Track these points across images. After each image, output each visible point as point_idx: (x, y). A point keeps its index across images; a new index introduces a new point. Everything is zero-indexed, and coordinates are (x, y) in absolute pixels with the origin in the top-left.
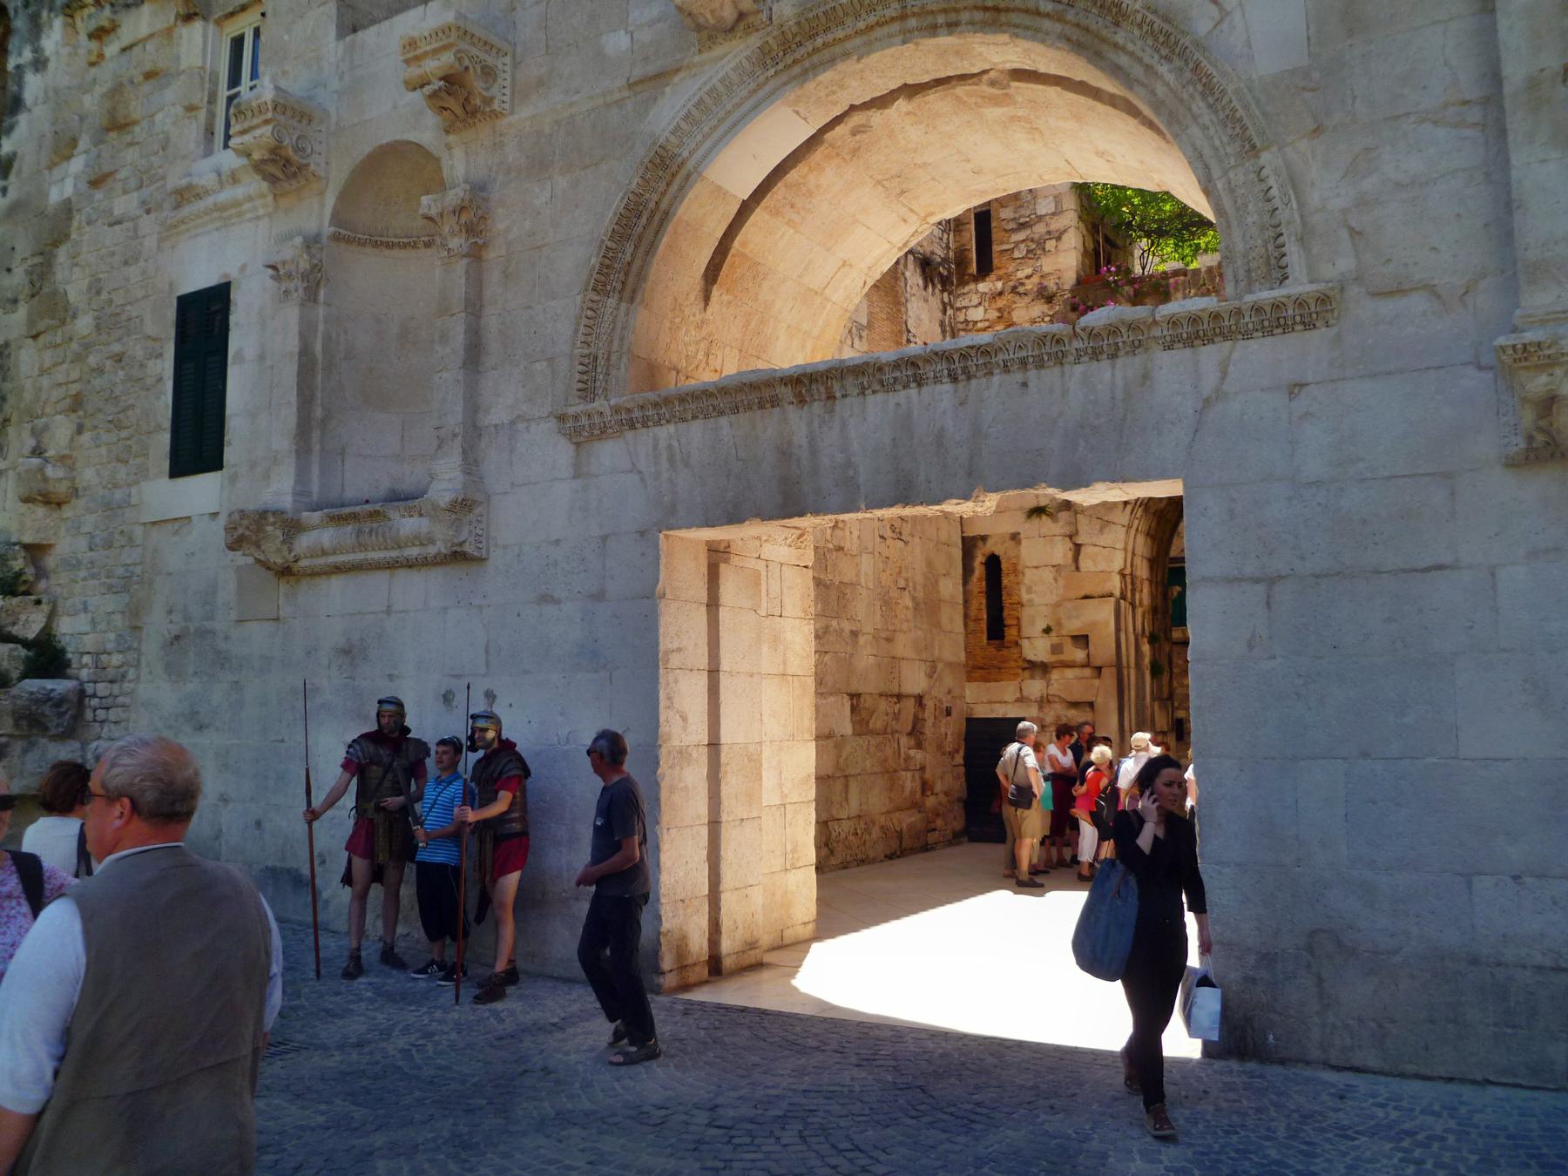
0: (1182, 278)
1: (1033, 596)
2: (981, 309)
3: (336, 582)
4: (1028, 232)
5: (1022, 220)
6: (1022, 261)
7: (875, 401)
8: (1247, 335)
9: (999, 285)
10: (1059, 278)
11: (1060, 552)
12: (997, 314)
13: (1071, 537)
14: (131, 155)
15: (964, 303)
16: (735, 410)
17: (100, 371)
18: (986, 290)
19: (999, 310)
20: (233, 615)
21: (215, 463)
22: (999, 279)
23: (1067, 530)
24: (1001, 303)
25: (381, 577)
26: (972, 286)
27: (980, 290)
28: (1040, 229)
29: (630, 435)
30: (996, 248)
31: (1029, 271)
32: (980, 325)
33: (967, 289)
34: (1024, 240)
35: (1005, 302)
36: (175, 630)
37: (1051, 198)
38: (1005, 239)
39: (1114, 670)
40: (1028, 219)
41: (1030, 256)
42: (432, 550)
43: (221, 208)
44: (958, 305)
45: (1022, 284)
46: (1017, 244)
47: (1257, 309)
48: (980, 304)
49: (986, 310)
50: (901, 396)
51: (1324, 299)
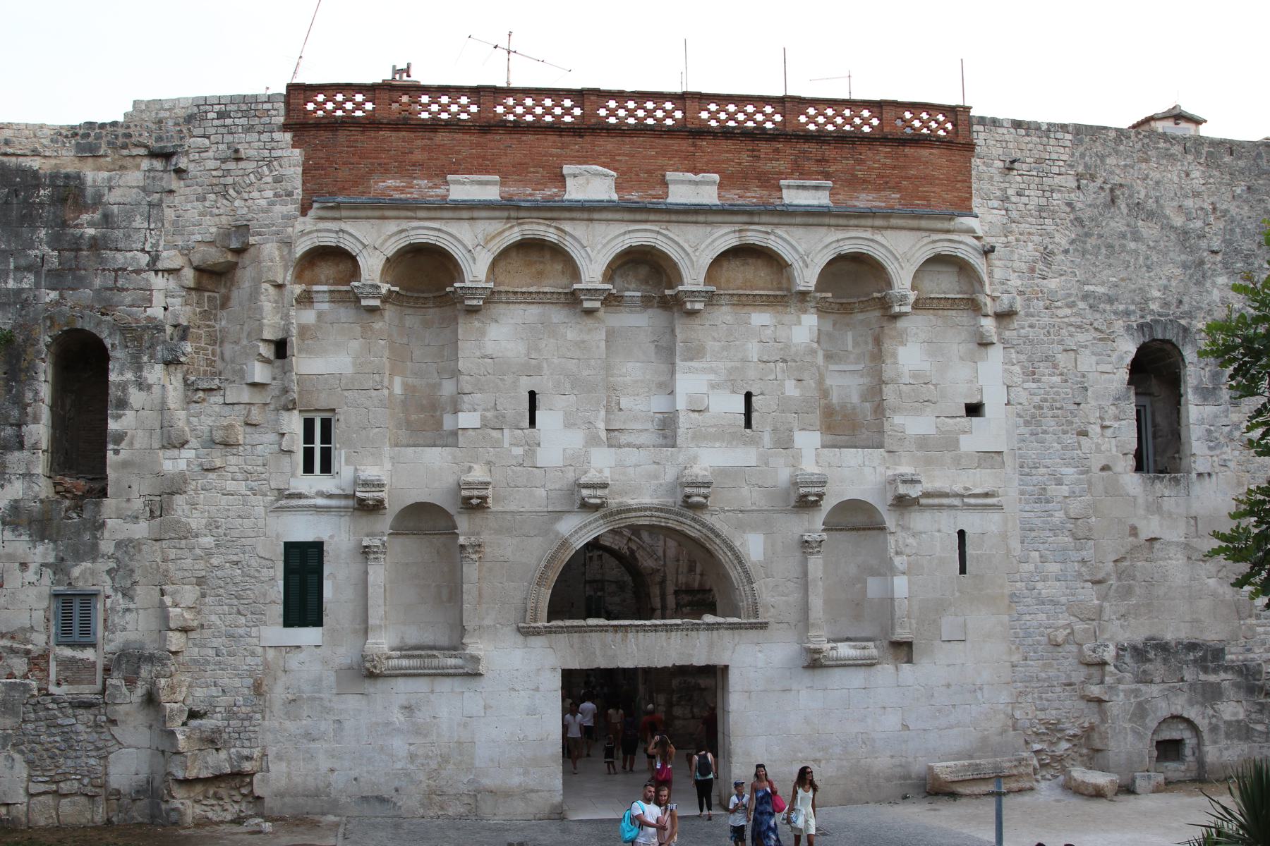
3: (400, 681)
7: (641, 635)
8: (746, 629)
14: (233, 460)
16: (591, 631)
17: (219, 567)
20: (334, 691)
21: (319, 623)
25: (426, 679)
36: (291, 697)
42: (461, 671)
43: (316, 506)
47: (750, 624)
50: (650, 634)
51: (766, 623)
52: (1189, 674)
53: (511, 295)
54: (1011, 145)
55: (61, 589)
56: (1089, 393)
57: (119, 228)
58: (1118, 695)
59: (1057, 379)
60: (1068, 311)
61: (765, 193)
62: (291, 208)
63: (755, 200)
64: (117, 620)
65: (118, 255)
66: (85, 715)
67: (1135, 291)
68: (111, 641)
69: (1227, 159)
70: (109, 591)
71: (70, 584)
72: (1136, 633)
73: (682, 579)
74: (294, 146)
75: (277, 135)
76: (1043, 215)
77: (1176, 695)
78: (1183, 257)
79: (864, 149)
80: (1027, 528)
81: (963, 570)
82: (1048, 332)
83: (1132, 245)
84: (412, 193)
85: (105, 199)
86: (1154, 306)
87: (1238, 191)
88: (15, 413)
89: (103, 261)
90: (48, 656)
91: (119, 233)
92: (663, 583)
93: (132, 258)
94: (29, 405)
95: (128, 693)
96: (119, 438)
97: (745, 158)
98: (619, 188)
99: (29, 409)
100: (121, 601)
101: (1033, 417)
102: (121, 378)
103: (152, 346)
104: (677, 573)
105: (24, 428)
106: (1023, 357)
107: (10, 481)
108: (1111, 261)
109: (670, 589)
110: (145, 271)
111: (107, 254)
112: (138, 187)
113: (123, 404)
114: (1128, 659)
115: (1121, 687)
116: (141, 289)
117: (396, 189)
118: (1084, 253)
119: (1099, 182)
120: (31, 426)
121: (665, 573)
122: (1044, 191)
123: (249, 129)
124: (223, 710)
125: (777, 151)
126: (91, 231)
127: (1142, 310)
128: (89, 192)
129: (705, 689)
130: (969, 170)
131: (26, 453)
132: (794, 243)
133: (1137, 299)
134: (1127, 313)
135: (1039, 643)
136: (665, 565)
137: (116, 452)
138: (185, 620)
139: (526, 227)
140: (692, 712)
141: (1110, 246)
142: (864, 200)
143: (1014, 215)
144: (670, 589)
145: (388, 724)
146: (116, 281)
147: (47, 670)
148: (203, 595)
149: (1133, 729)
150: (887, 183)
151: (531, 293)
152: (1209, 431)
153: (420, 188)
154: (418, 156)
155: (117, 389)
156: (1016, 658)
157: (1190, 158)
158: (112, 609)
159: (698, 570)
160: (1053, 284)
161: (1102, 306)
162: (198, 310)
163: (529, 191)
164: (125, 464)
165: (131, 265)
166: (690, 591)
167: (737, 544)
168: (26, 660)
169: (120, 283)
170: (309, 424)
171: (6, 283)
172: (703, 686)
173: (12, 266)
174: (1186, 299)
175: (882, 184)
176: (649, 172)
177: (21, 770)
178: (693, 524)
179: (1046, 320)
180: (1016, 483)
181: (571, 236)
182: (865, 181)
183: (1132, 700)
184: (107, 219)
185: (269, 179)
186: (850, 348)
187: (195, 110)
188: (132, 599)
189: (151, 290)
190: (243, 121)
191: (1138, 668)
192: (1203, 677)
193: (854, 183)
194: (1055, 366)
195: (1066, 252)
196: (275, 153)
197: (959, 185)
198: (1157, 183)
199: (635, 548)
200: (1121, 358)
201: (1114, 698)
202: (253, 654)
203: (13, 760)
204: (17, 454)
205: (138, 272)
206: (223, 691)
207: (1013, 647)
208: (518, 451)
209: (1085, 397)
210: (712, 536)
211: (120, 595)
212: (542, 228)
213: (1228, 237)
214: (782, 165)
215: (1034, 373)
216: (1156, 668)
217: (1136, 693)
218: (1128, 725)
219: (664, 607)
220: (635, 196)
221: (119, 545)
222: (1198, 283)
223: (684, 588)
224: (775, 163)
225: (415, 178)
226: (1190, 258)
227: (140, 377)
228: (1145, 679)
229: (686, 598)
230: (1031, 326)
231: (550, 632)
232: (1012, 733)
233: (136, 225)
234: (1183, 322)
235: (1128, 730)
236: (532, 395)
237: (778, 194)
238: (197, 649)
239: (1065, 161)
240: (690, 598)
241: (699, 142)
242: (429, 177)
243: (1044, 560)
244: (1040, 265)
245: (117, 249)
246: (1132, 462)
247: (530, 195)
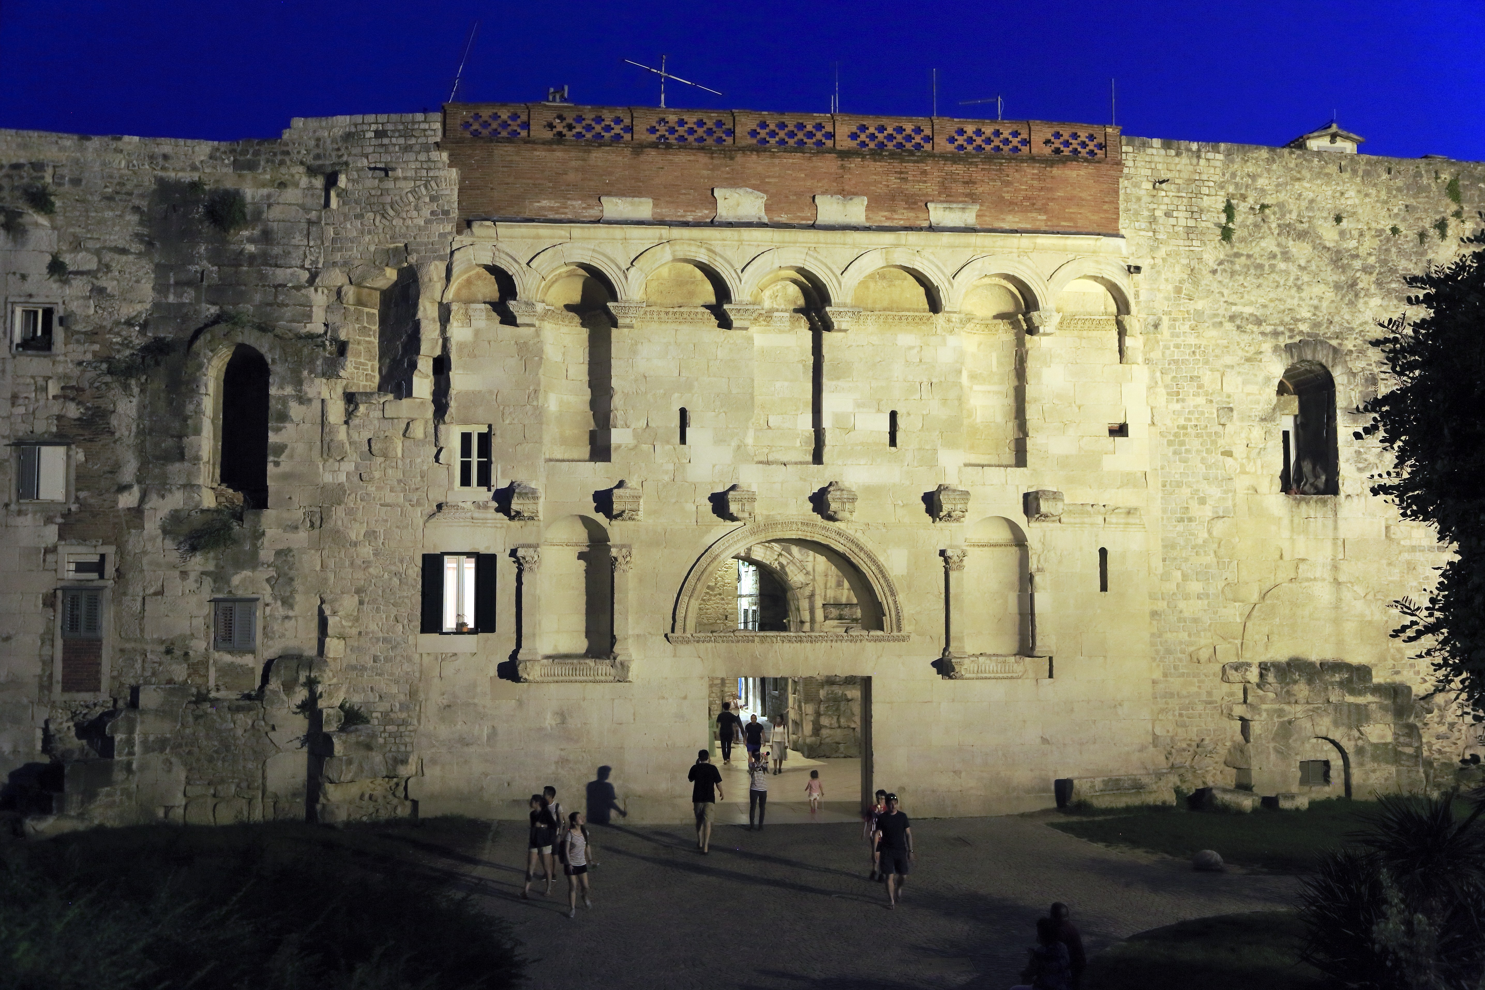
7: (787, 645)
29: (696, 644)
36: (445, 702)
50: (795, 644)
52: (1335, 696)
53: (663, 315)
54: (1159, 166)
55: (220, 596)
56: (1235, 413)
57: (278, 244)
58: (1259, 714)
59: (1201, 400)
60: (1214, 333)
61: (912, 215)
62: (449, 228)
63: (902, 222)
64: (276, 628)
65: (279, 271)
66: (244, 720)
67: (1284, 311)
68: (269, 647)
69: (1385, 176)
70: (268, 599)
71: (230, 592)
72: (1281, 653)
73: (831, 593)
74: (450, 166)
75: (435, 155)
76: (1191, 236)
77: (1321, 716)
78: (1335, 278)
79: (1011, 171)
80: (1169, 546)
81: (1104, 588)
82: (1194, 352)
83: (1282, 266)
84: (565, 213)
85: (264, 216)
86: (1304, 327)
87: (1396, 211)
88: (176, 425)
89: (263, 277)
90: (207, 662)
91: (276, 250)
92: (812, 596)
93: (292, 274)
94: (190, 417)
95: (285, 698)
96: (280, 449)
97: (893, 181)
98: (768, 208)
99: (190, 422)
100: (280, 609)
101: (1176, 435)
102: (280, 393)
103: (312, 361)
105: (185, 440)
106: (1168, 378)
107: (170, 491)
108: (1260, 281)
109: (819, 602)
110: (305, 287)
111: (268, 270)
112: (298, 205)
113: (283, 417)
114: (1271, 678)
115: (1264, 707)
116: (301, 305)
117: (551, 209)
118: (1233, 273)
119: (1251, 201)
120: (192, 438)
122: (1192, 212)
123: (407, 149)
124: (379, 715)
125: (924, 173)
126: (251, 248)
127: (1291, 330)
128: (249, 210)
130: (1117, 192)
131: (186, 464)
132: (940, 265)
133: (1287, 319)
134: (1276, 334)
135: (1180, 660)
136: (814, 580)
137: (277, 464)
138: (343, 627)
139: (677, 247)
141: (1260, 267)
142: (1010, 221)
143: (1161, 236)
144: (819, 602)
145: (541, 729)
146: (276, 297)
147: (206, 676)
148: (361, 603)
149: (1276, 750)
150: (1034, 204)
151: (682, 313)
152: (1358, 453)
153: (574, 208)
154: (571, 177)
155: (277, 403)
156: (1157, 675)
157: (1346, 176)
158: (270, 615)
160: (1200, 305)
161: (1250, 326)
162: (357, 326)
163: (681, 212)
164: (286, 477)
165: (291, 281)
166: (837, 605)
167: (881, 559)
168: (186, 666)
169: (281, 298)
170: (466, 438)
171: (166, 297)
172: (849, 696)
173: (172, 281)
174: (1337, 319)
175: (1030, 204)
176: (796, 194)
177: (180, 774)
178: (837, 537)
179: (1192, 340)
180: (1159, 500)
181: (721, 257)
182: (1011, 203)
183: (1276, 720)
184: (267, 236)
185: (427, 200)
186: (995, 369)
187: (353, 130)
188: (291, 607)
189: (311, 307)
190: (402, 141)
191: (1282, 688)
192: (1350, 699)
193: (1002, 205)
194: (1200, 387)
195: (1214, 272)
196: (431, 174)
197: (1105, 207)
198: (1312, 201)
199: (785, 563)
200: (1268, 380)
201: (1256, 717)
202: (409, 659)
203: (171, 763)
204: (177, 466)
205: (298, 288)
206: (380, 697)
207: (1154, 664)
208: (671, 467)
209: (1231, 418)
210: (857, 550)
211: (279, 603)
212: (693, 249)
213: (1383, 257)
214: (930, 187)
215: (1178, 393)
216: (1301, 690)
217: (1280, 713)
218: (1272, 745)
219: (813, 620)
220: (784, 218)
221: (279, 553)
222: (1351, 303)
224: (922, 186)
225: (569, 199)
226: (1343, 278)
227: (300, 391)
228: (1288, 697)
229: (834, 612)
230: (1177, 346)
231: (698, 642)
232: (1151, 749)
233: (295, 241)
234: (1334, 343)
235: (1271, 750)
236: (683, 412)
237: (925, 216)
238: (354, 656)
239: (1215, 182)
241: (847, 164)
242: (583, 198)
243: (1185, 578)
244: (1186, 286)
245: (277, 266)
246: (1278, 484)
247: (682, 216)
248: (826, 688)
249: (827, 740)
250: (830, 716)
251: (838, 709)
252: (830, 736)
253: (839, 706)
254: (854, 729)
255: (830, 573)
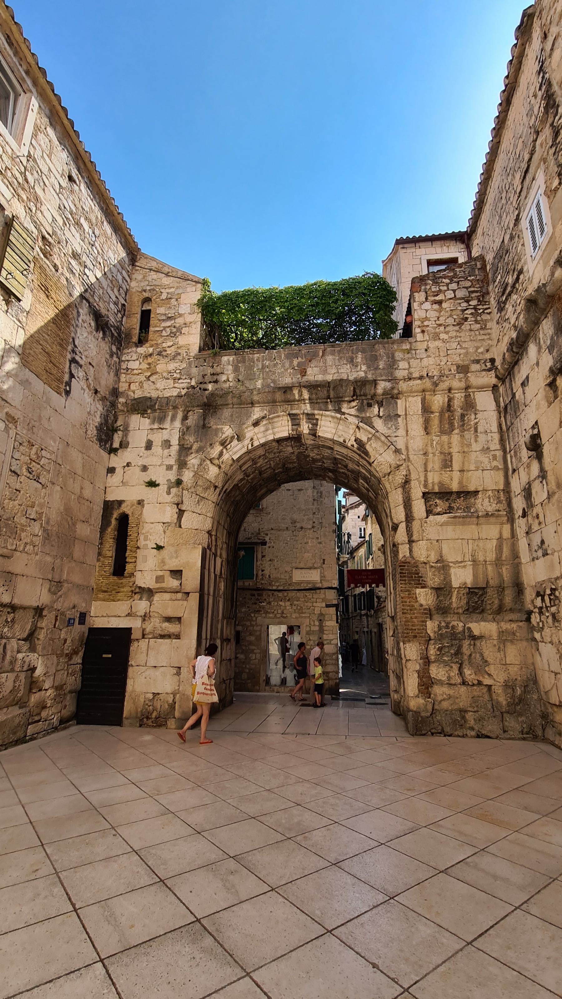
0: (262, 354)
1: (148, 542)
2: (138, 362)
4: (173, 322)
5: (169, 315)
6: (167, 338)
9: (151, 350)
10: (188, 349)
11: (170, 514)
12: (148, 367)
13: (178, 504)
15: (127, 358)
18: (142, 352)
19: (149, 364)
22: (151, 346)
23: (176, 500)
24: (150, 360)
26: (134, 349)
27: (139, 352)
28: (179, 321)
30: (151, 329)
31: (170, 344)
32: (135, 372)
33: (130, 350)
34: (169, 326)
35: (153, 360)
37: (189, 305)
38: (158, 325)
39: (198, 595)
40: (173, 315)
41: (172, 335)
44: (123, 359)
45: (166, 351)
46: (165, 328)
48: (137, 359)
49: (140, 363)
73: (434, 478)
92: (407, 482)
104: (426, 471)
109: (417, 492)
121: (409, 471)
129: (481, 637)
140: (461, 673)
144: (417, 492)
159: (456, 466)
172: (476, 632)
199: (364, 439)
219: (409, 518)
223: (436, 489)
229: (441, 505)
240: (447, 504)
248: (437, 618)
249: (445, 705)
250: (446, 664)
251: (458, 652)
252: (450, 697)
253: (460, 647)
254: (489, 687)
255: (430, 450)
